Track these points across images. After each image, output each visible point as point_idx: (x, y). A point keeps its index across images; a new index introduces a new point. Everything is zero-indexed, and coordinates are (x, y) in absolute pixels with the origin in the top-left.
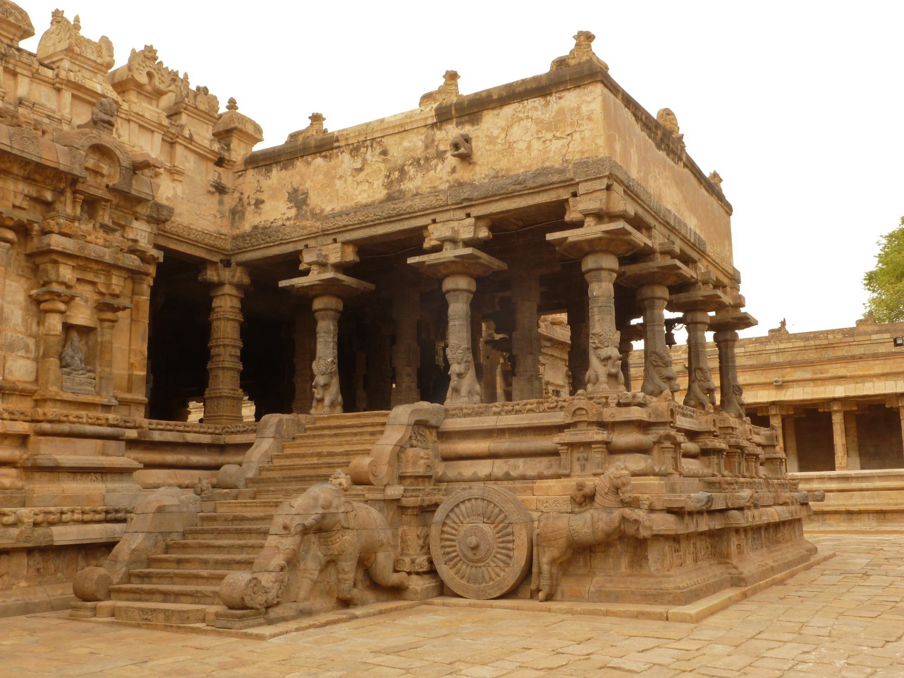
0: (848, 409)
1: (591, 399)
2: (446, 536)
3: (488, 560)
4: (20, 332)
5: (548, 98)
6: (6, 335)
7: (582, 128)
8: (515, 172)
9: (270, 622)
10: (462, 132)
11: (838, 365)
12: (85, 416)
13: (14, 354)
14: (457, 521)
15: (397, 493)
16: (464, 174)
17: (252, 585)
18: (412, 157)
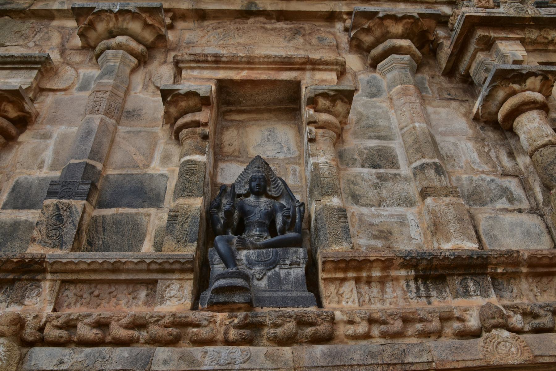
4: (483, 172)
13: (488, 208)
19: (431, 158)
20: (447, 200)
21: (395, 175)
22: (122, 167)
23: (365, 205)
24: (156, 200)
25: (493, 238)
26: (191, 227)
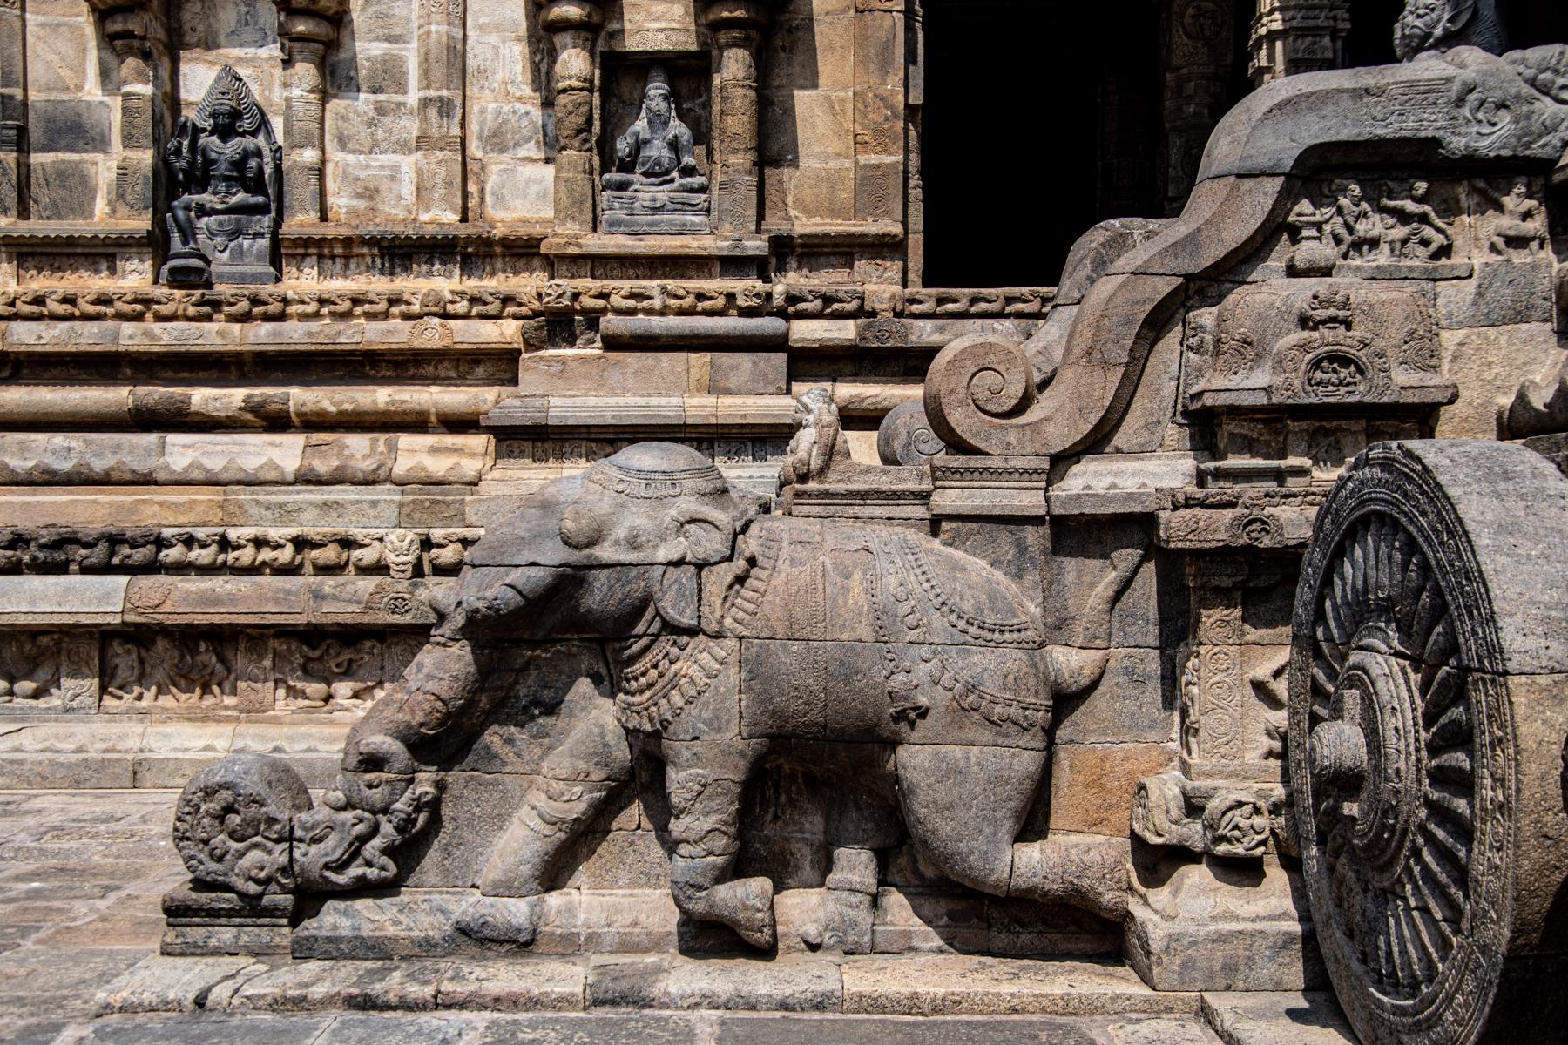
4: (519, 99)
6: (483, 111)
9: (303, 951)
12: (656, 292)
13: (506, 157)
15: (1130, 485)
17: (213, 806)
19: (438, 89)
20: (440, 155)
21: (399, 104)
22: (49, 89)
23: (353, 152)
24: (99, 143)
25: (499, 198)
26: (141, 189)
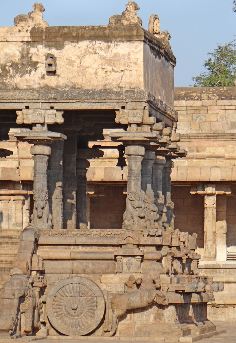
0: (222, 192)
1: (133, 231)
2: (56, 303)
3: (82, 315)
5: (109, 44)
7: (130, 69)
8: (87, 88)
10: (49, 52)
11: (216, 143)
14: (63, 295)
16: (52, 81)
18: (12, 62)
